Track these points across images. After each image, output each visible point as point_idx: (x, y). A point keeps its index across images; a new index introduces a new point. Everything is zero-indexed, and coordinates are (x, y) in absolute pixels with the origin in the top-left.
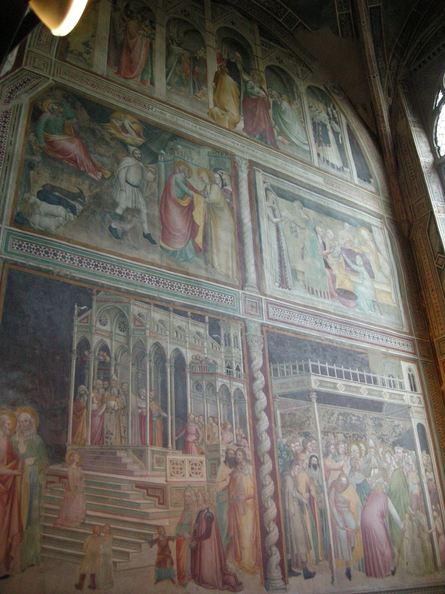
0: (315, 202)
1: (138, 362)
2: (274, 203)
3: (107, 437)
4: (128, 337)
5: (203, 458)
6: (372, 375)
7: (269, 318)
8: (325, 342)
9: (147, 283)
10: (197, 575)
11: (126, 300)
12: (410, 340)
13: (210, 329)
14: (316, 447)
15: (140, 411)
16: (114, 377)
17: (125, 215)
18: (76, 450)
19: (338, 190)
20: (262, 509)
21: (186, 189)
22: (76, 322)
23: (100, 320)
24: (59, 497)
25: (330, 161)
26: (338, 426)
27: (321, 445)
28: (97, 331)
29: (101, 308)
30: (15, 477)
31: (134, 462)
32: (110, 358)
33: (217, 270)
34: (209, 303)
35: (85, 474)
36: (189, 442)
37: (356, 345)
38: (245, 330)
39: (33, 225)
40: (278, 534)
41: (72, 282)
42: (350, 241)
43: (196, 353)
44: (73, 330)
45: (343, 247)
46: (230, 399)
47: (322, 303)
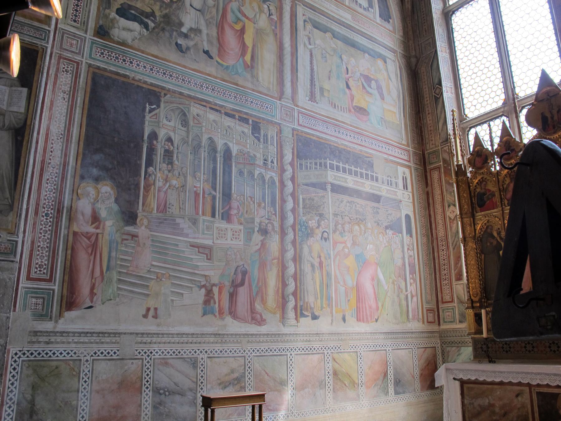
0: (343, 35)
1: (195, 152)
2: (310, 32)
3: (169, 208)
4: (188, 132)
5: (241, 227)
6: (375, 175)
8: (341, 147)
9: (204, 90)
10: (233, 312)
11: (187, 102)
13: (252, 130)
15: (195, 189)
16: (176, 162)
17: (189, 34)
18: (145, 216)
19: (362, 26)
20: (283, 268)
21: (240, 16)
23: (166, 118)
24: (131, 251)
25: (358, 1)
27: (331, 224)
30: (98, 234)
32: (174, 147)
34: (253, 109)
35: (151, 235)
36: (231, 215)
37: (365, 151)
38: (280, 131)
39: (112, 37)
41: (144, 86)
42: (368, 69)
43: (241, 147)
44: (144, 124)
45: (362, 73)
46: (265, 185)
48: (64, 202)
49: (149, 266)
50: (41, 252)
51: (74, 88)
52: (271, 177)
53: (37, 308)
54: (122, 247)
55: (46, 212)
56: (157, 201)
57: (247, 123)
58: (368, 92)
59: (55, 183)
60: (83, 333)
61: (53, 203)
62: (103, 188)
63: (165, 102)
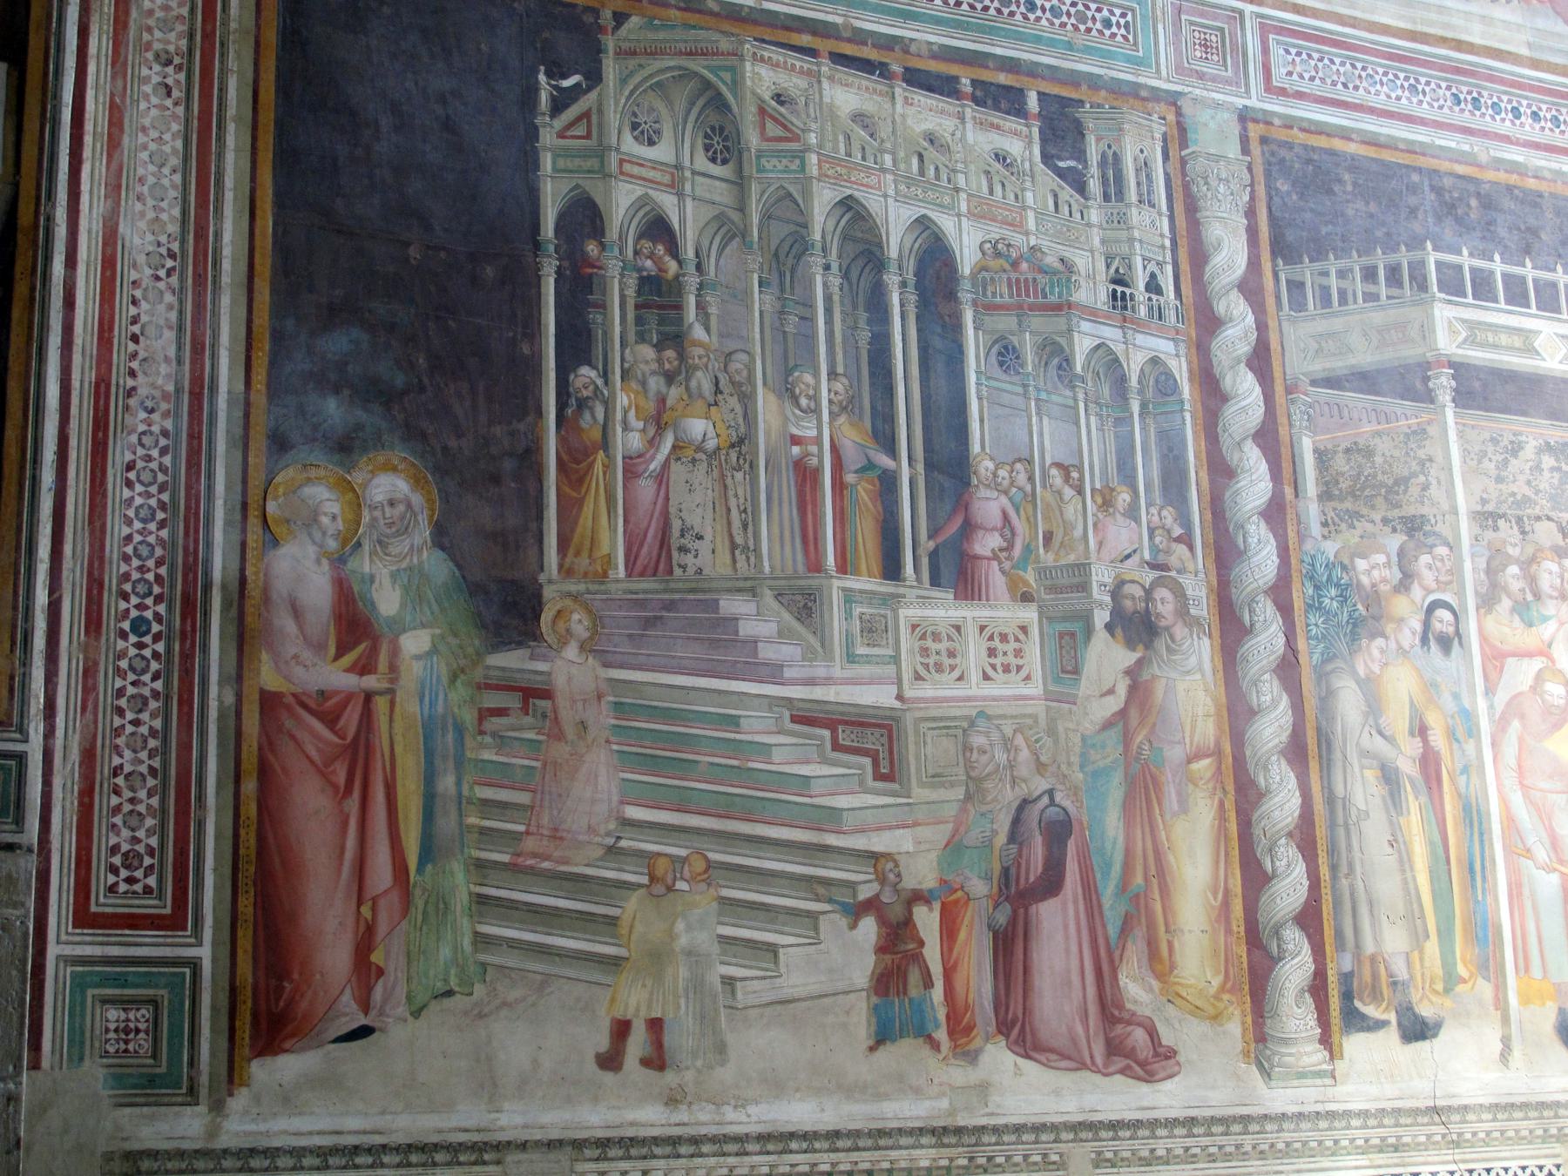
3: (683, 550)
4: (740, 183)
5: (1030, 614)
7: (1269, 88)
8: (1490, 175)
10: (1014, 1023)
11: (725, 44)
13: (1044, 141)
14: (1450, 572)
15: (796, 450)
16: (699, 333)
18: (575, 597)
22: (547, 137)
23: (635, 126)
24: (526, 762)
26: (1537, 492)
27: (1468, 565)
28: (627, 167)
29: (637, 79)
30: (368, 697)
31: (784, 634)
32: (680, 263)
36: (977, 557)
38: (1181, 133)
40: (1306, 883)
43: (996, 232)
44: (537, 166)
46: (1126, 400)
47: (1485, 20)
48: (208, 562)
49: (612, 826)
50: (127, 794)
51: (208, 36)
52: (1155, 361)
53: (131, 1047)
54: (482, 746)
55: (134, 613)
56: (626, 521)
57: (1020, 111)
59: (161, 478)
60: (335, 1150)
61: (163, 571)
62: (375, 481)
63: (622, 54)
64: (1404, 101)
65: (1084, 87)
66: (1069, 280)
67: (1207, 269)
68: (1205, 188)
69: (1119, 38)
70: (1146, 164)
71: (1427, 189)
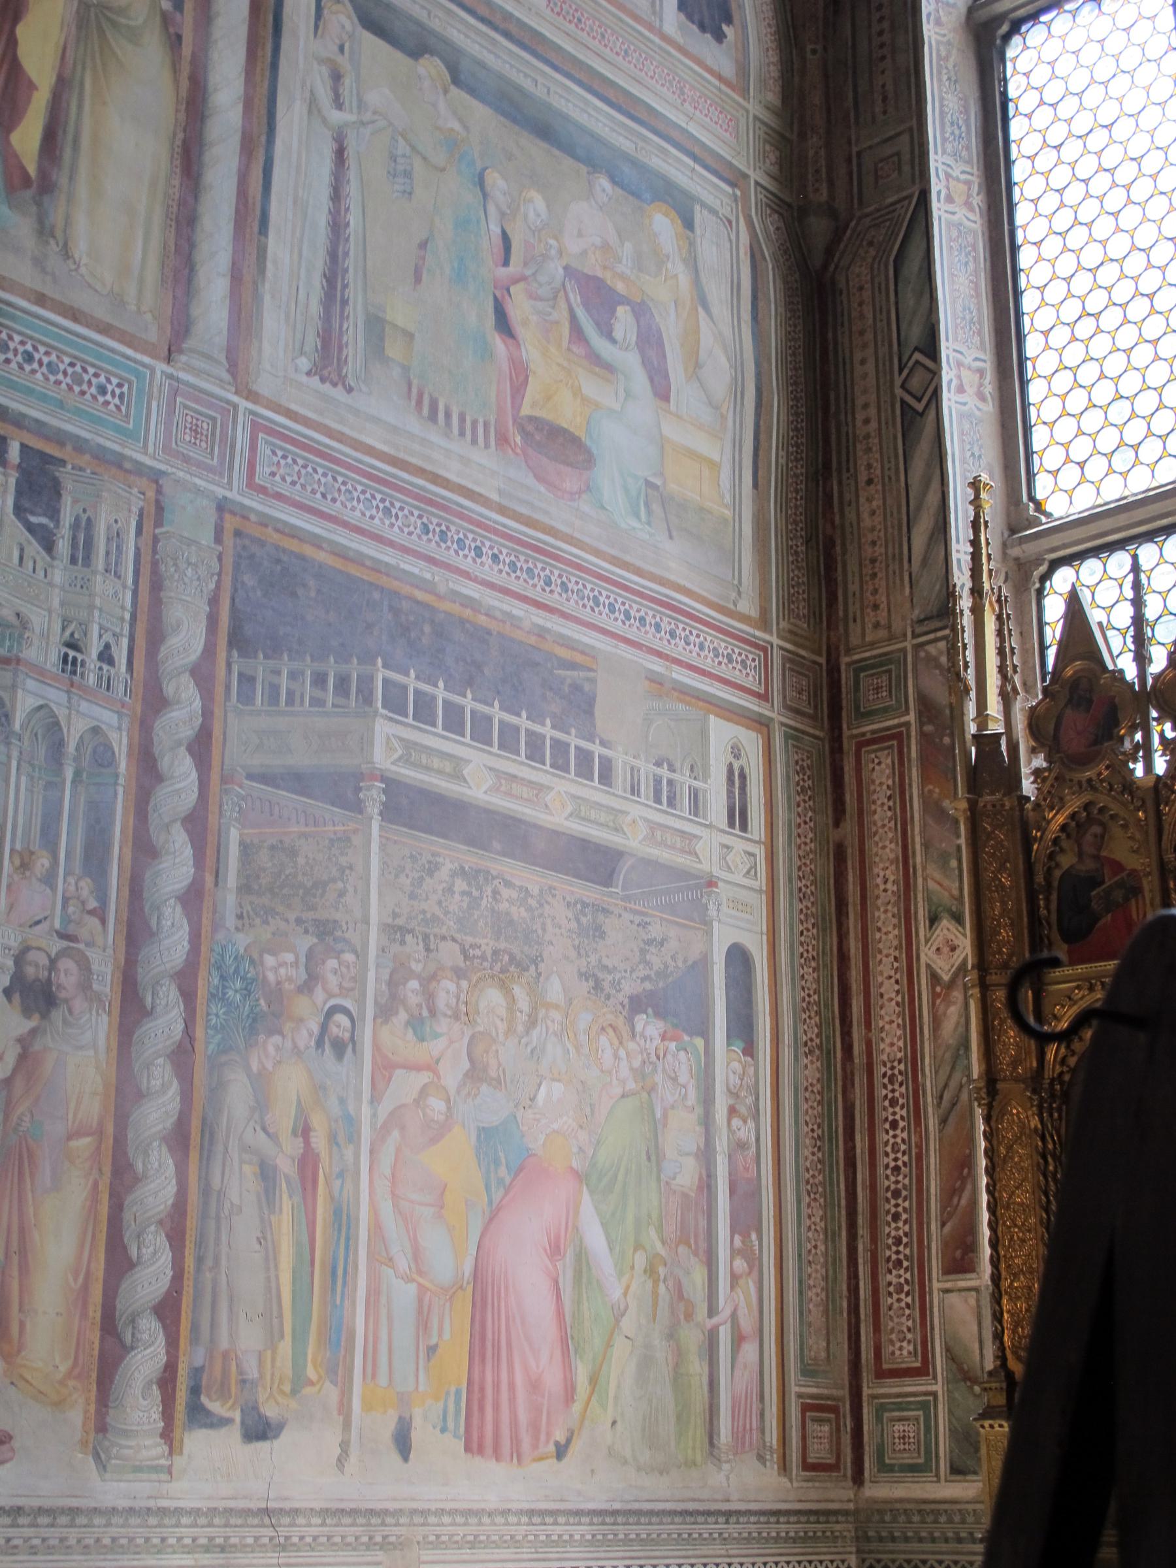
0: (501, 77)
2: (341, 49)
6: (597, 749)
7: (251, 483)
12: (756, 646)
13: (19, 493)
14: (354, 979)
26: (446, 913)
27: (371, 975)
33: (83, 270)
34: (30, 392)
37: (562, 636)
40: (170, 1273)
42: (606, 247)
52: (96, 730)
58: (595, 359)
64: (377, 521)
65: (69, 448)
66: (21, 636)
67: (162, 649)
68: (172, 569)
69: (112, 407)
70: (118, 534)
71: (386, 608)
